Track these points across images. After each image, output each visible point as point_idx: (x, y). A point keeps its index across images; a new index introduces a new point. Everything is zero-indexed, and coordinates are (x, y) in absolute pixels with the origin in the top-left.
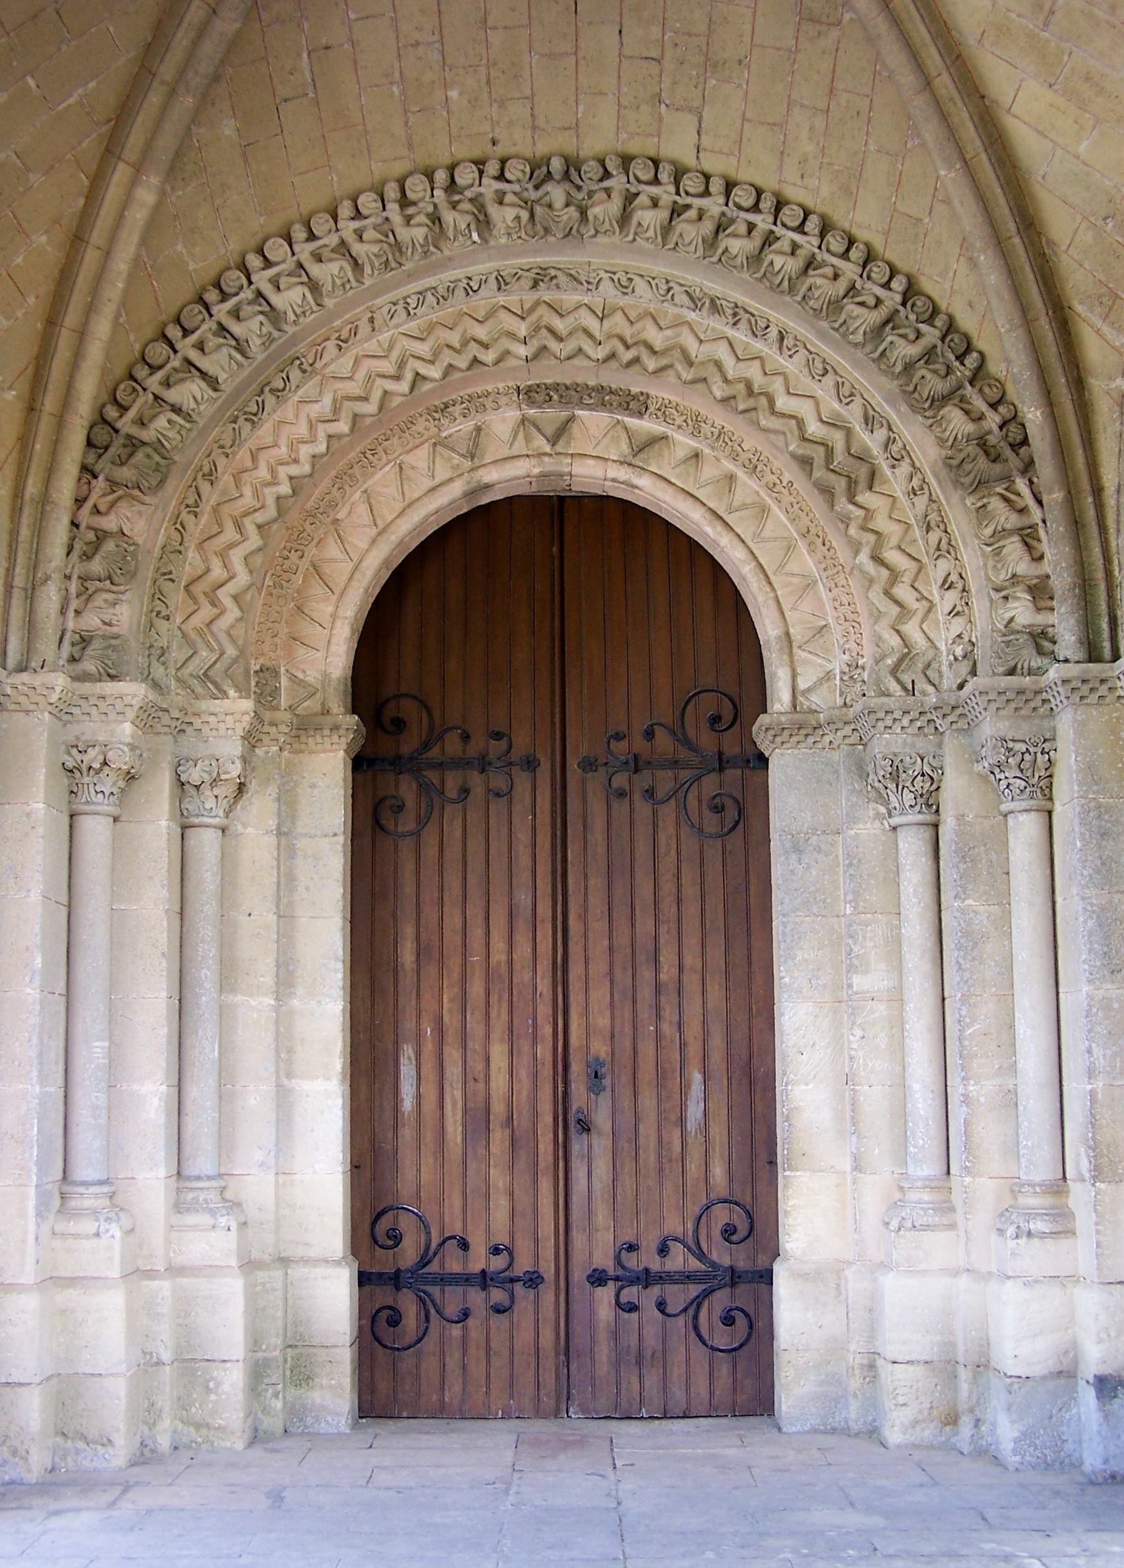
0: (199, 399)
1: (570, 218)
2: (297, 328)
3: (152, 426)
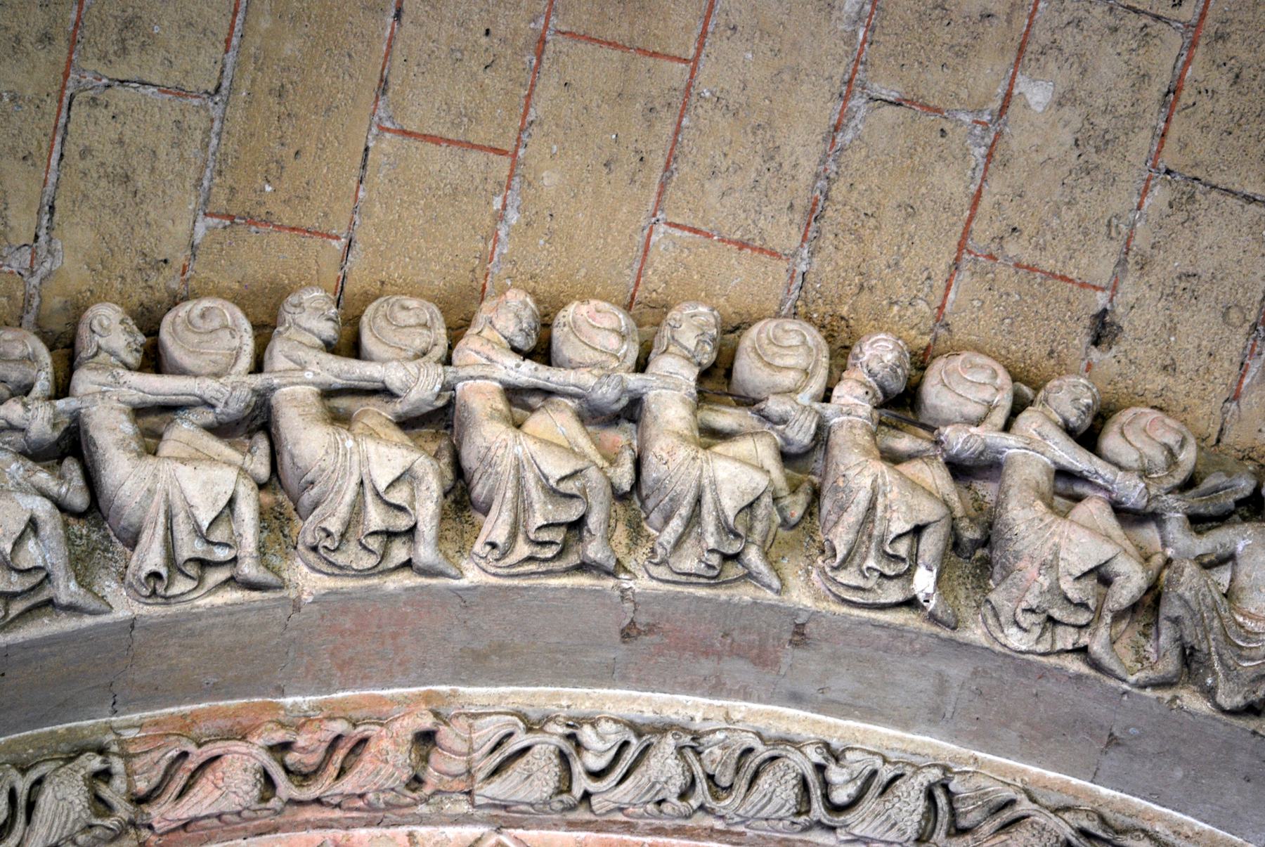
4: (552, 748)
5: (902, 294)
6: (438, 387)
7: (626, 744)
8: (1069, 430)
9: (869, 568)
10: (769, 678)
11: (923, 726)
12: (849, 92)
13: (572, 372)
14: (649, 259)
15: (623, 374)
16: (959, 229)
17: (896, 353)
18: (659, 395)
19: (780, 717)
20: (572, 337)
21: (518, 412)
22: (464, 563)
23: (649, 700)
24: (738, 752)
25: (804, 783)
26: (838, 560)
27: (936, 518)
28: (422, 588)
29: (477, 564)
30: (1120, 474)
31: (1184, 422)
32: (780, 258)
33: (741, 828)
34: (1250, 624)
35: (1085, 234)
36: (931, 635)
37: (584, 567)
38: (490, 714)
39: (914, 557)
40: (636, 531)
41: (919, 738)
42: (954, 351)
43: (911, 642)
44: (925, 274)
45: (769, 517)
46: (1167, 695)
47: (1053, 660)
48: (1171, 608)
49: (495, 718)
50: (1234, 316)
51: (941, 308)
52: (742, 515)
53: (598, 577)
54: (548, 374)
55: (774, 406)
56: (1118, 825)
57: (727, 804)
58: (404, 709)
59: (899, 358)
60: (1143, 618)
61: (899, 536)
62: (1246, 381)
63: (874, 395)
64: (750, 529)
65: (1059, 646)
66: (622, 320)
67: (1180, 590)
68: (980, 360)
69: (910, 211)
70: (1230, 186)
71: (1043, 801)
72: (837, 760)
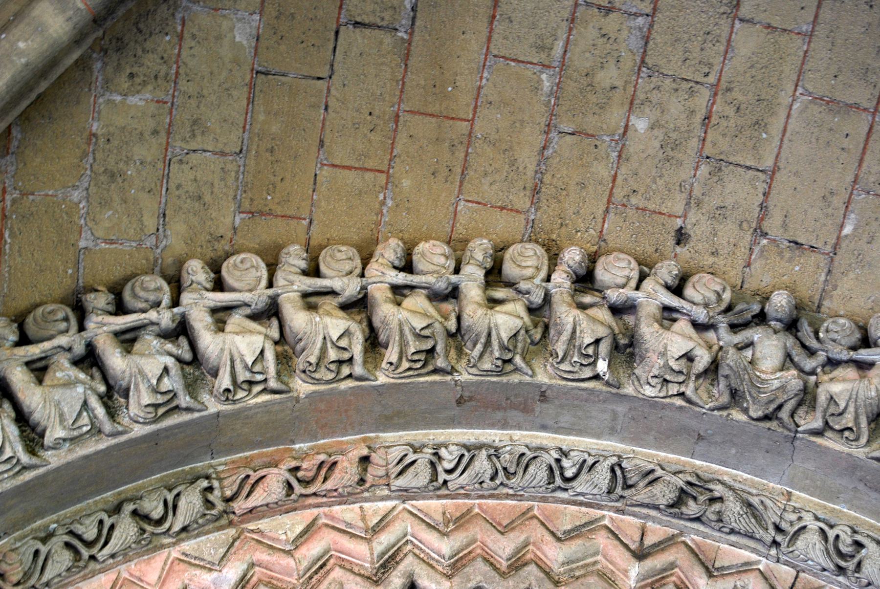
1: (783, 388)
4: (427, 460)
5: (582, 226)
6: (359, 288)
7: (462, 456)
8: (668, 287)
9: (575, 362)
10: (530, 418)
11: (607, 437)
12: (549, 130)
13: (424, 277)
14: (457, 218)
15: (448, 276)
16: (607, 193)
17: (581, 256)
18: (467, 284)
19: (537, 437)
20: (422, 259)
21: (399, 298)
22: (378, 373)
23: (472, 433)
24: (518, 456)
25: (551, 469)
26: (559, 359)
27: (606, 335)
28: (358, 387)
30: (694, 307)
31: (724, 279)
32: (521, 213)
33: (522, 493)
34: (763, 376)
35: (669, 191)
36: (607, 392)
37: (436, 371)
38: (395, 446)
39: (596, 355)
40: (460, 351)
41: (605, 443)
42: (609, 252)
43: (598, 396)
44: (592, 216)
45: (524, 340)
46: (725, 413)
47: (668, 400)
48: (724, 371)
49: (398, 447)
50: (745, 225)
51: (601, 232)
52: (511, 340)
53: (443, 376)
54: (412, 278)
55: (523, 286)
56: (705, 478)
57: (514, 481)
58: (354, 446)
59: (582, 258)
60: (711, 376)
61: (588, 345)
62: (753, 257)
63: (572, 277)
64: (515, 347)
65: (670, 393)
66: (446, 249)
67: (728, 362)
68: (622, 256)
69: (582, 185)
70: (738, 162)
71: (668, 469)
72: (566, 456)
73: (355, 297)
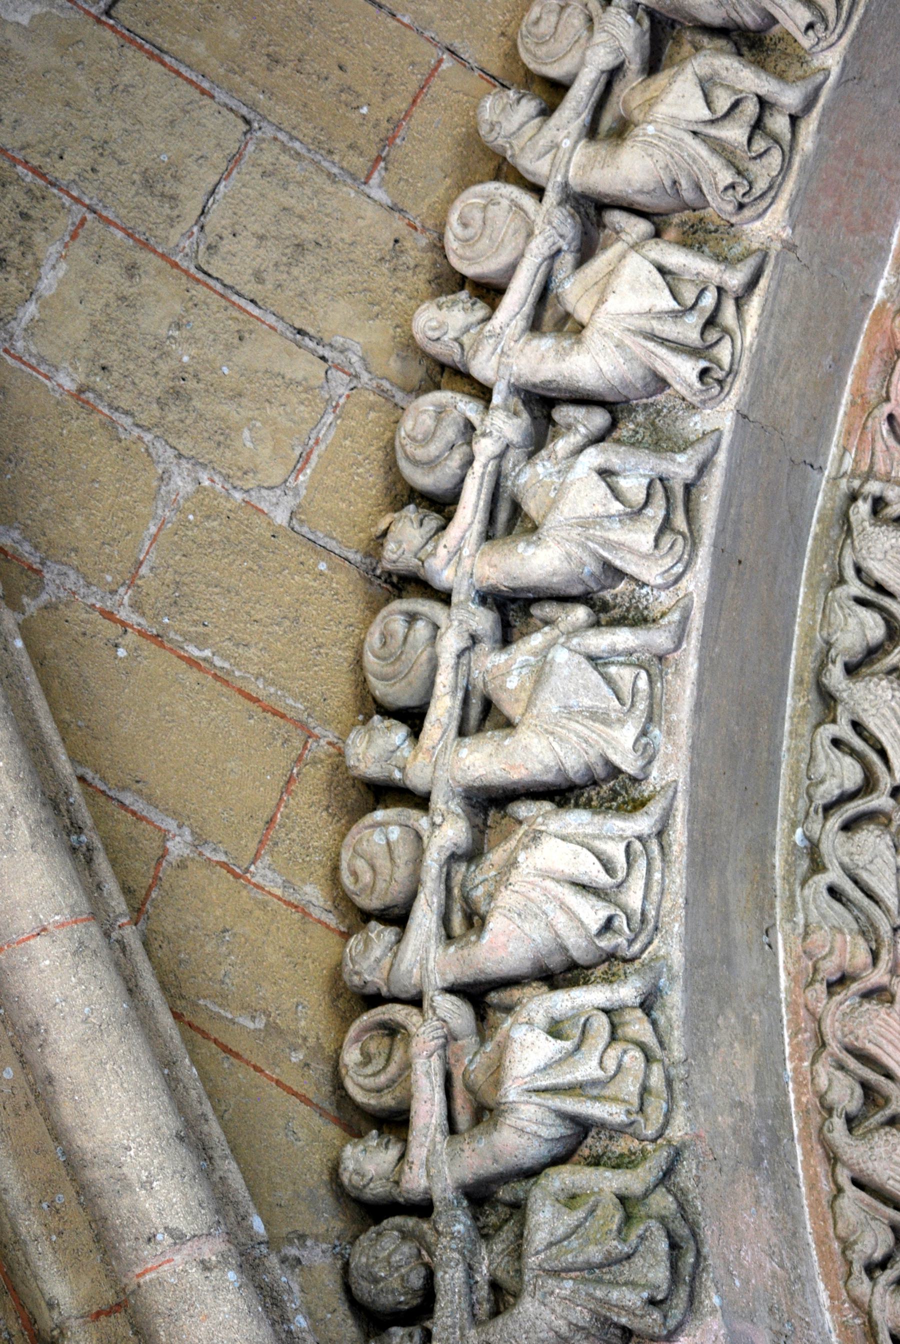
0: (602, 879)
2: (738, 388)
3: (512, 1092)
6: (629, 19)
22: (816, 63)
28: (823, 114)
29: (822, 51)
73: (643, 33)
